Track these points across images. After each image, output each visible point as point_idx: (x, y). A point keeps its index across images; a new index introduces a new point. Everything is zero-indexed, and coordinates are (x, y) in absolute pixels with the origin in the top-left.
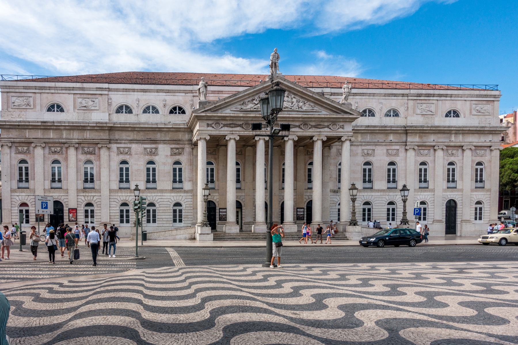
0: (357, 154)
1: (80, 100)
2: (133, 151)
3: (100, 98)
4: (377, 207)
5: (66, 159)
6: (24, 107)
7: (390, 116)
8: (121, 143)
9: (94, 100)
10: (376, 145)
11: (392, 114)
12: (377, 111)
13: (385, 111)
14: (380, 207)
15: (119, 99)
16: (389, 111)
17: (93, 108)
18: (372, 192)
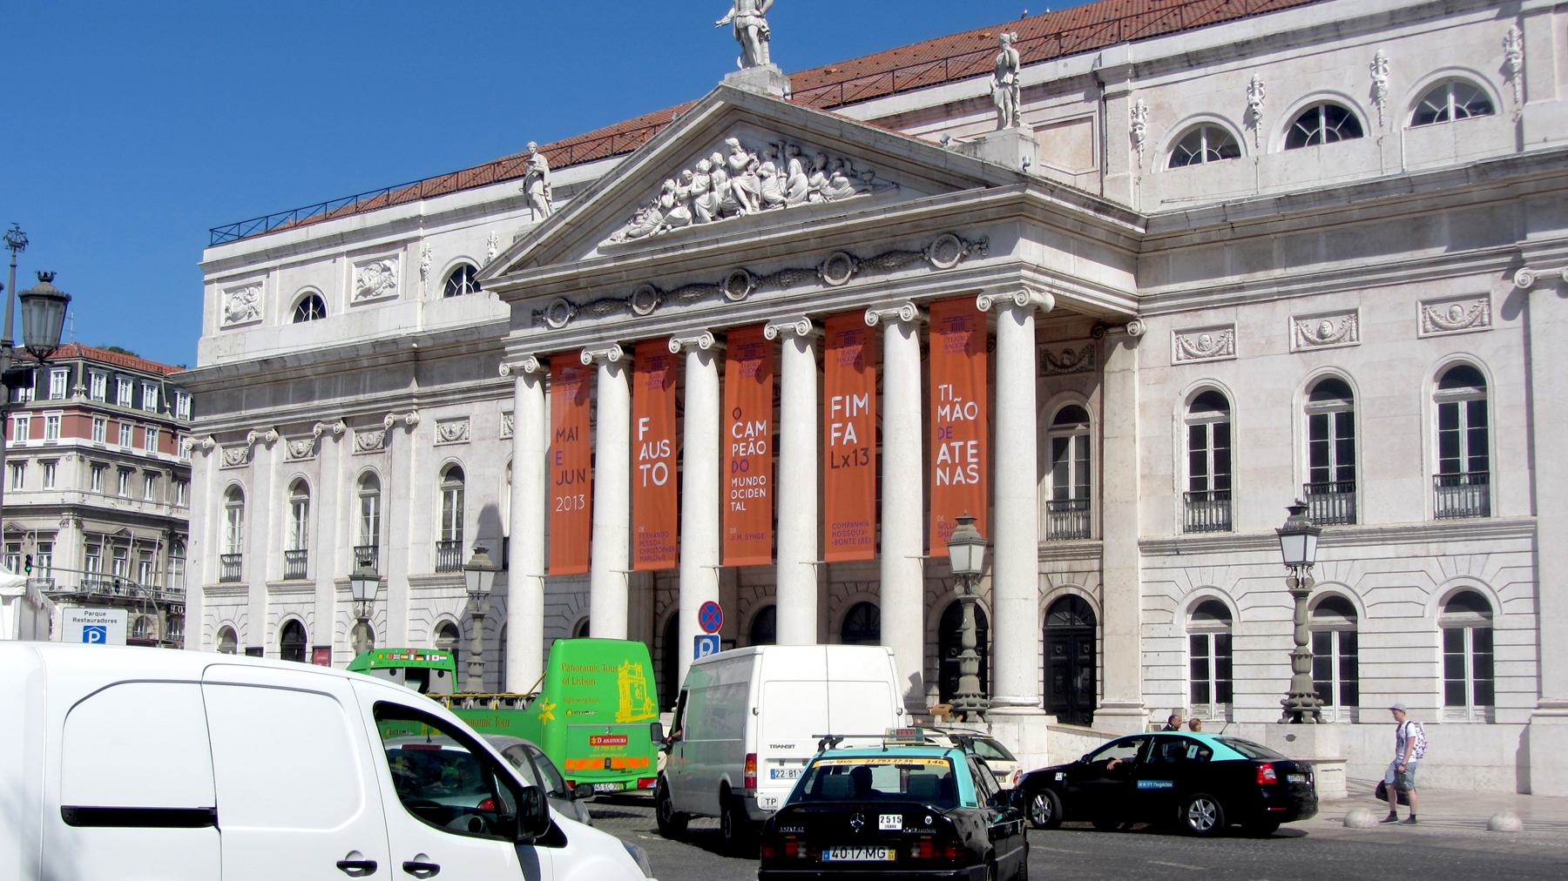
0: (1269, 342)
1: (356, 272)
2: (471, 430)
3: (400, 252)
4: (1381, 626)
5: (318, 476)
6: (245, 320)
7: (1444, 116)
8: (444, 403)
9: (387, 263)
10: (1362, 286)
11: (1451, 103)
12: (1359, 104)
13: (1400, 94)
14: (1394, 625)
15: (444, 248)
16: (1436, 92)
17: (388, 292)
18: (1346, 540)
